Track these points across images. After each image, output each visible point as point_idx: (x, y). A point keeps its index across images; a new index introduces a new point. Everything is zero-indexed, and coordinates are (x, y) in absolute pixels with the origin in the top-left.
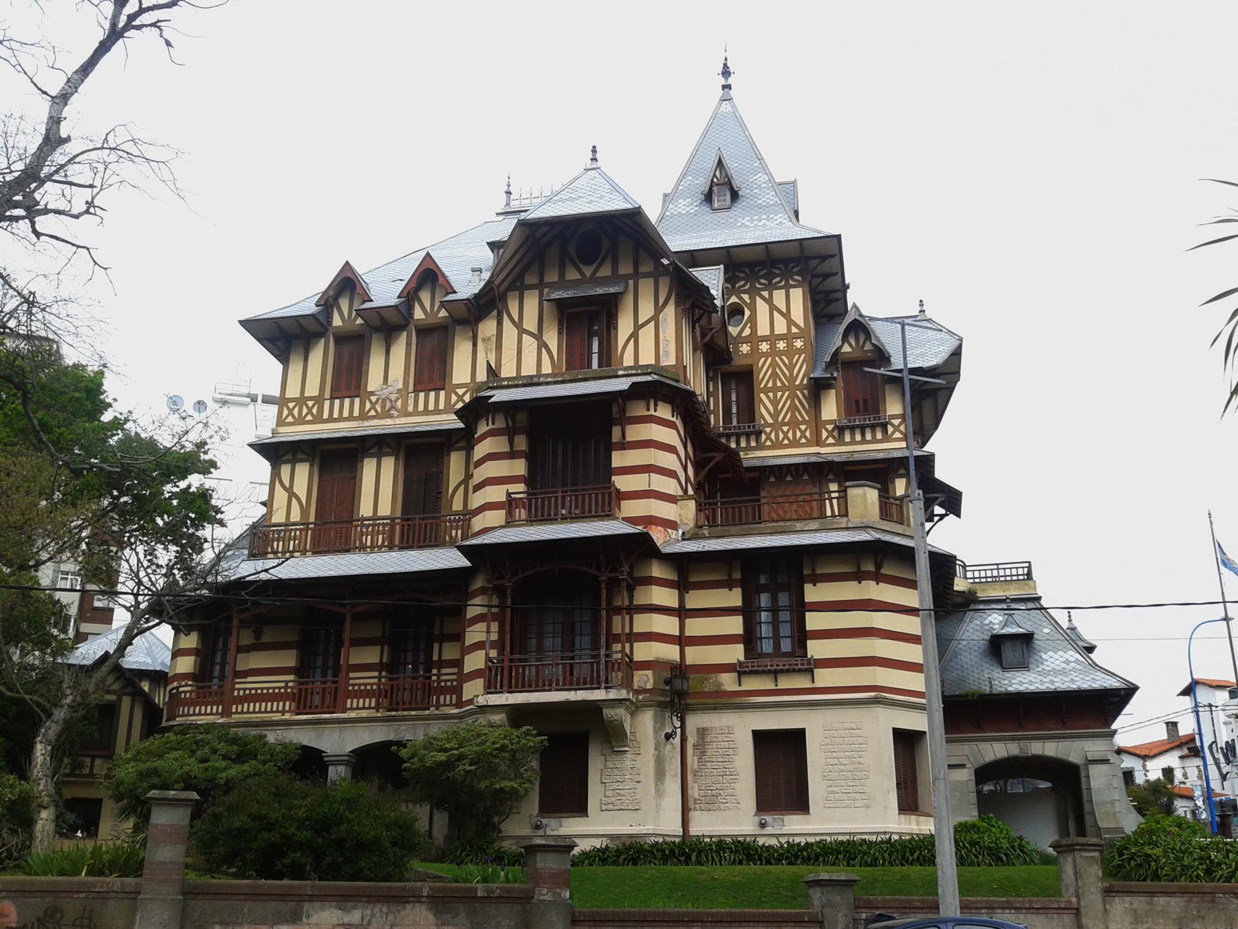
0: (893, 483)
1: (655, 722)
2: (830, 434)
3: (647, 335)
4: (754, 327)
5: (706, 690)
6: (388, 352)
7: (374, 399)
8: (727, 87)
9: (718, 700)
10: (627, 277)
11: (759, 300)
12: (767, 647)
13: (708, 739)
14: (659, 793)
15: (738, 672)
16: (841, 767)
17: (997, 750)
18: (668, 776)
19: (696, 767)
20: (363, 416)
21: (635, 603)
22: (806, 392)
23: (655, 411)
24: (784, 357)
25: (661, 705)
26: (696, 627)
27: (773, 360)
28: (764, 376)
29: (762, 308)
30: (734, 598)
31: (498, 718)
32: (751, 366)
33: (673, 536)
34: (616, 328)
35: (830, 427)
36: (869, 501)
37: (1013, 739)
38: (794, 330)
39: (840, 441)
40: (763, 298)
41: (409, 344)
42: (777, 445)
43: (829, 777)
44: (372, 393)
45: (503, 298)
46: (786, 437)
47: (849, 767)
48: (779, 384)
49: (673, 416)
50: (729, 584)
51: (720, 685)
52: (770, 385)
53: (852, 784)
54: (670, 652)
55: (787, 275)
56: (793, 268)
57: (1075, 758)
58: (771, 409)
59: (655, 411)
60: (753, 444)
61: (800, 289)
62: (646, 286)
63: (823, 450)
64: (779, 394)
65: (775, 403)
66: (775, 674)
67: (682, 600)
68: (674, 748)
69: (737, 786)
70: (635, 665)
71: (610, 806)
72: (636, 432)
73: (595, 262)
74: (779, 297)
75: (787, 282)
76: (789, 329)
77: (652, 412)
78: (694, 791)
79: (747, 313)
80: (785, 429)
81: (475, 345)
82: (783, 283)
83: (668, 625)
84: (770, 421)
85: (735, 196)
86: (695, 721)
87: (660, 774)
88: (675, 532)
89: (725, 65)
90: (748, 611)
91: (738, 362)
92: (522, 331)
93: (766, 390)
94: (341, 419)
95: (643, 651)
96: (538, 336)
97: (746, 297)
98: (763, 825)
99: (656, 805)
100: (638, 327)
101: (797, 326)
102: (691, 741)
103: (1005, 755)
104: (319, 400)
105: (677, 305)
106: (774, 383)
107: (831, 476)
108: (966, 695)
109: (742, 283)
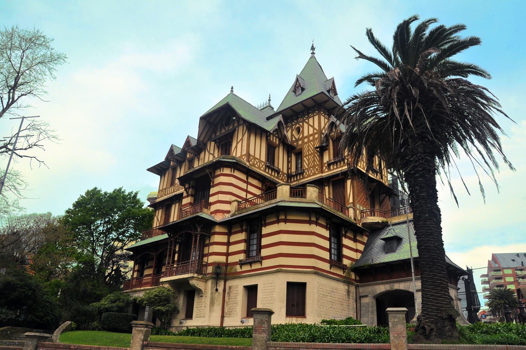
0: (346, 182)
1: (212, 285)
2: (326, 167)
3: (239, 145)
4: (303, 134)
5: (232, 272)
6: (180, 170)
7: (176, 185)
8: (313, 53)
9: (235, 276)
10: (236, 127)
11: (305, 124)
12: (254, 253)
13: (231, 290)
14: (211, 311)
15: (240, 264)
16: (267, 299)
17: (381, 288)
18: (216, 304)
19: (227, 301)
20: (174, 192)
21: (211, 242)
22: (318, 153)
23: (223, 171)
24: (312, 142)
25: (213, 278)
26: (233, 248)
27: (309, 144)
28: (305, 152)
29: (306, 125)
30: (242, 236)
31: (166, 286)
32: (301, 149)
33: (227, 216)
34: (232, 146)
35: (326, 165)
36: (285, 190)
37: (387, 283)
38: (315, 131)
39: (329, 169)
40: (306, 122)
41: (185, 166)
42: (309, 176)
43: (263, 303)
44: (176, 184)
45: (205, 145)
46: (311, 172)
47: (269, 299)
48: (310, 153)
49: (231, 172)
50: (241, 232)
51: (236, 269)
52: (307, 154)
53: (269, 305)
54: (223, 259)
55: (313, 112)
57: (411, 290)
58: (307, 163)
59: (223, 171)
60: (301, 177)
62: (241, 128)
63: (323, 175)
64: (310, 156)
65: (308, 160)
66: (251, 264)
67: (229, 239)
68: (219, 294)
69: (237, 307)
70: (208, 265)
71: (198, 316)
72: (217, 180)
73: (228, 126)
74: (311, 120)
75: (313, 114)
76: (314, 131)
77: (222, 172)
78: (226, 310)
79: (301, 129)
80: (311, 169)
81: (199, 162)
83: (223, 249)
84: (307, 167)
86: (229, 283)
87: (212, 303)
88: (228, 214)
89: (313, 46)
90: (247, 241)
91: (299, 148)
92: (210, 154)
93: (306, 157)
94: (170, 194)
95: (212, 259)
96: (213, 154)
97: (301, 124)
98: (242, 322)
99: (209, 315)
100: (237, 143)
101: (316, 130)
102: (227, 291)
103: (384, 290)
104: (165, 189)
105: (248, 133)
106: (309, 153)
107: (326, 184)
108: (363, 266)
109: (300, 119)
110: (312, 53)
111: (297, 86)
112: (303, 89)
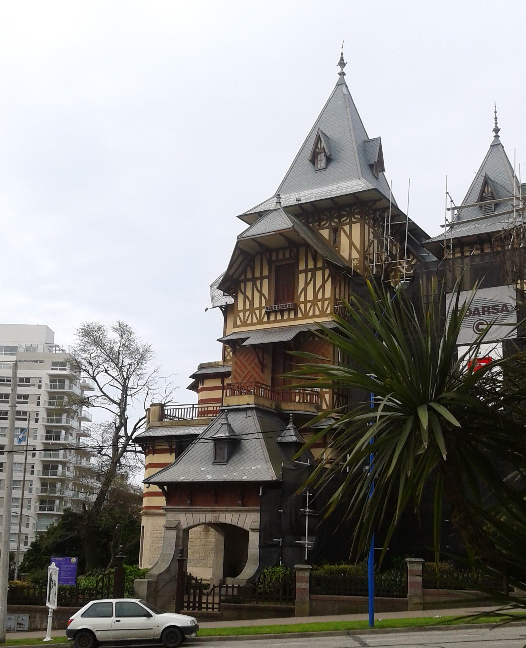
8: (342, 74)
55: (351, 215)
61: (359, 224)
82: (348, 220)
89: (342, 59)
110: (340, 74)
111: (317, 150)
112: (329, 160)
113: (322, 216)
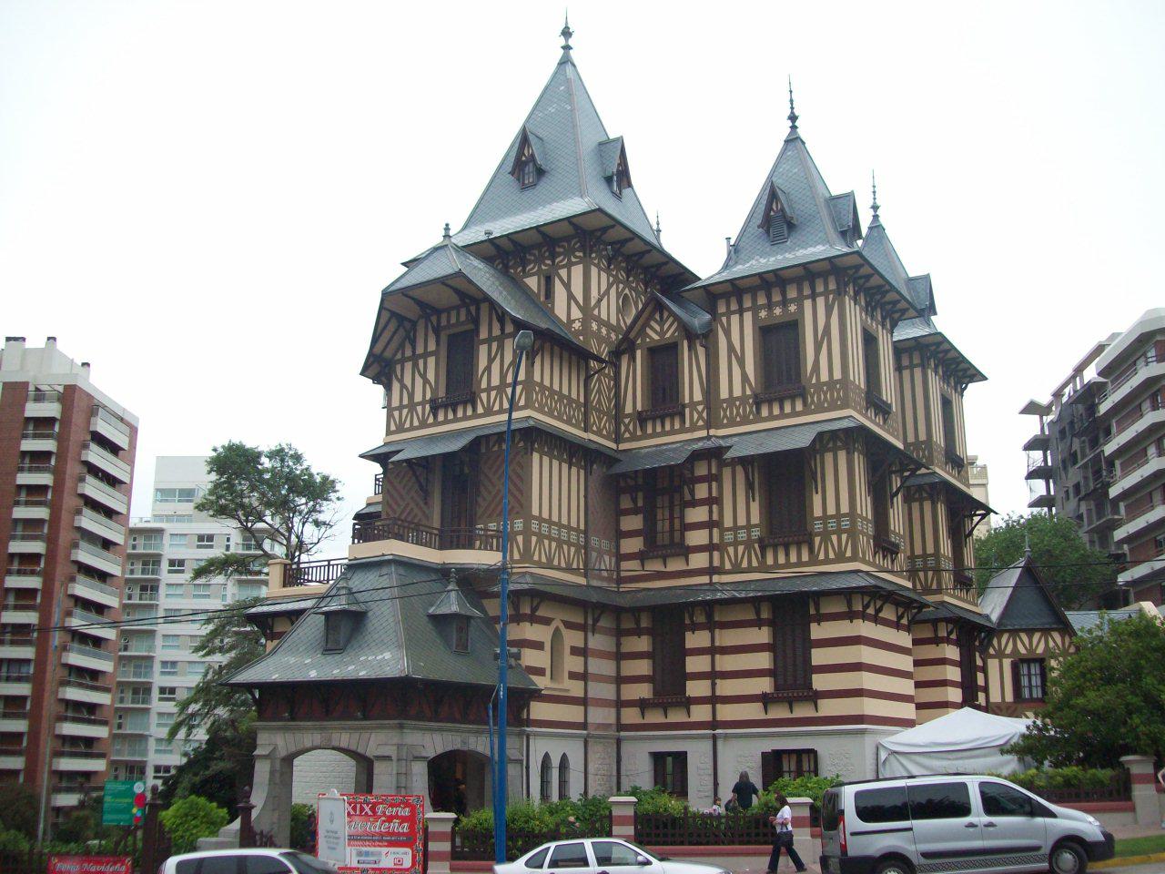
8: (567, 48)
56: (575, 244)
85: (540, 172)
89: (567, 28)
109: (532, 266)
110: (563, 48)
112: (540, 172)
113: (528, 257)
